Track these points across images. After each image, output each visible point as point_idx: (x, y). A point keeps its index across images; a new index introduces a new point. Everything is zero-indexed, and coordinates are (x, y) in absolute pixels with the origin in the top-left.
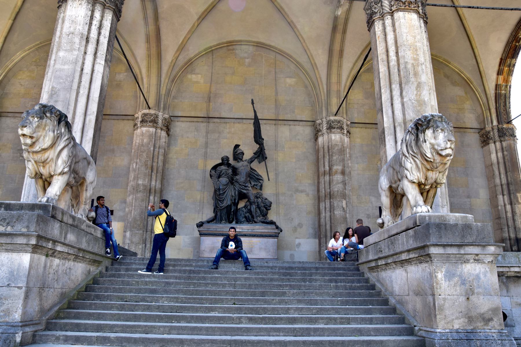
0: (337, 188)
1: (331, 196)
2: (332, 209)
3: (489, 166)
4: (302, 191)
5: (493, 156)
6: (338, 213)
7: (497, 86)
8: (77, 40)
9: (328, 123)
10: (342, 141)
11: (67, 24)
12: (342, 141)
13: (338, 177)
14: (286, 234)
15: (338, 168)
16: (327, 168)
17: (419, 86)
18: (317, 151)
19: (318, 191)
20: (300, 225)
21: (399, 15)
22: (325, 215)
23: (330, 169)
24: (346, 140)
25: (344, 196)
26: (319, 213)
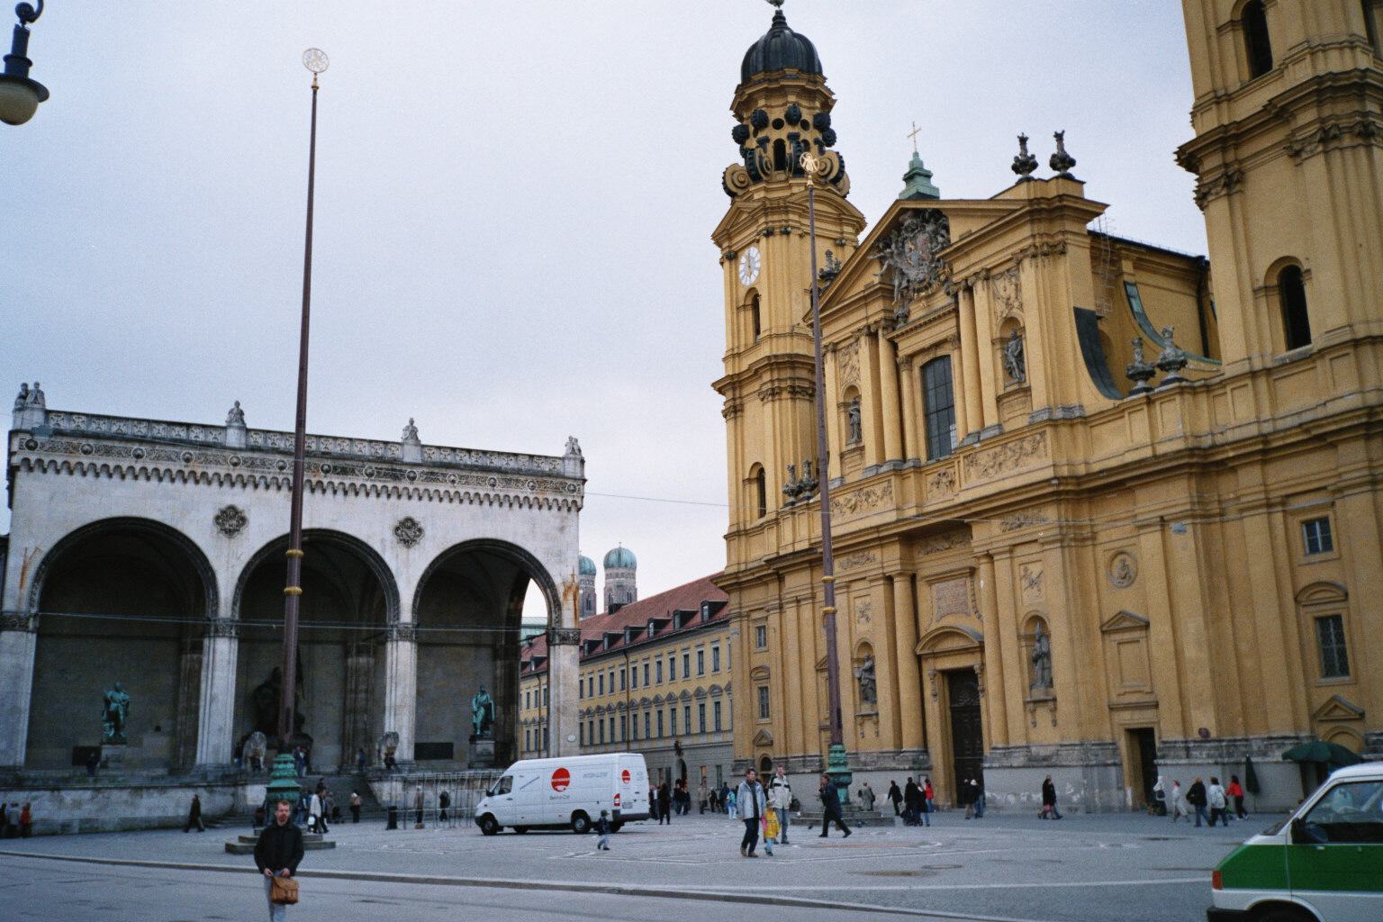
0: (361, 704)
1: (354, 711)
2: (355, 722)
3: (495, 678)
4: (331, 704)
5: (498, 672)
6: (360, 725)
7: (509, 611)
8: (225, 663)
9: (358, 647)
10: (368, 663)
11: (218, 657)
12: (368, 663)
13: (362, 696)
14: (317, 744)
15: (362, 687)
16: (353, 687)
17: (405, 688)
18: (346, 668)
19: (344, 704)
20: (327, 734)
21: (400, 643)
22: (349, 726)
23: (356, 687)
24: (372, 661)
25: (366, 711)
26: (344, 723)
